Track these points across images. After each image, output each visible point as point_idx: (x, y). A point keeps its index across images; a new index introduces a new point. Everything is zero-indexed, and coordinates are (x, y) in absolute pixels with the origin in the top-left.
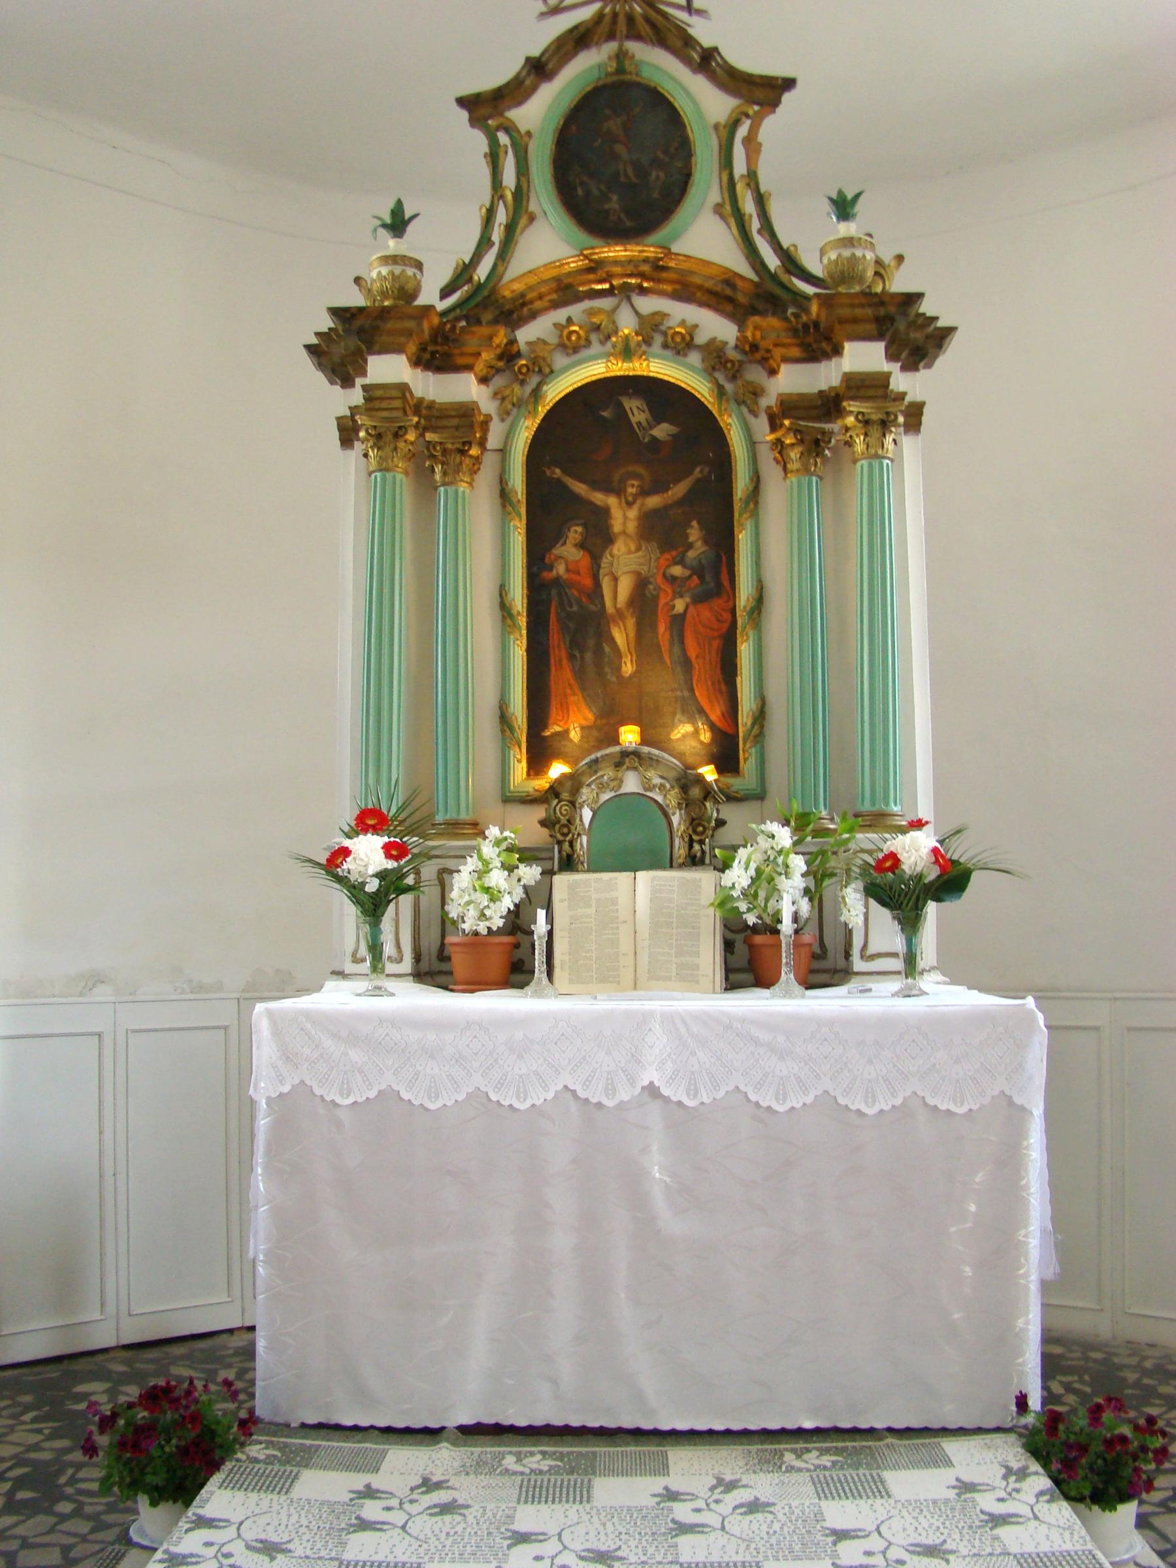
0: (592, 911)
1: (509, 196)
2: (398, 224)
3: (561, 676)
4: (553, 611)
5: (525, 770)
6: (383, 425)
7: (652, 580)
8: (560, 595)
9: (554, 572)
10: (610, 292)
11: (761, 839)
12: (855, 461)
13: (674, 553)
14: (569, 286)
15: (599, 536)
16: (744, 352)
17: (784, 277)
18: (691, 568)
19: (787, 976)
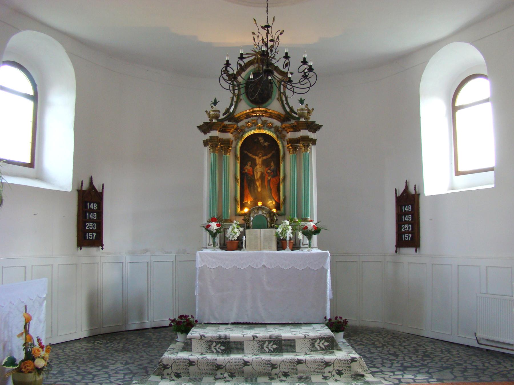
2: (215, 103)
3: (247, 191)
6: (212, 143)
15: (254, 165)
17: (290, 113)
19: (288, 247)
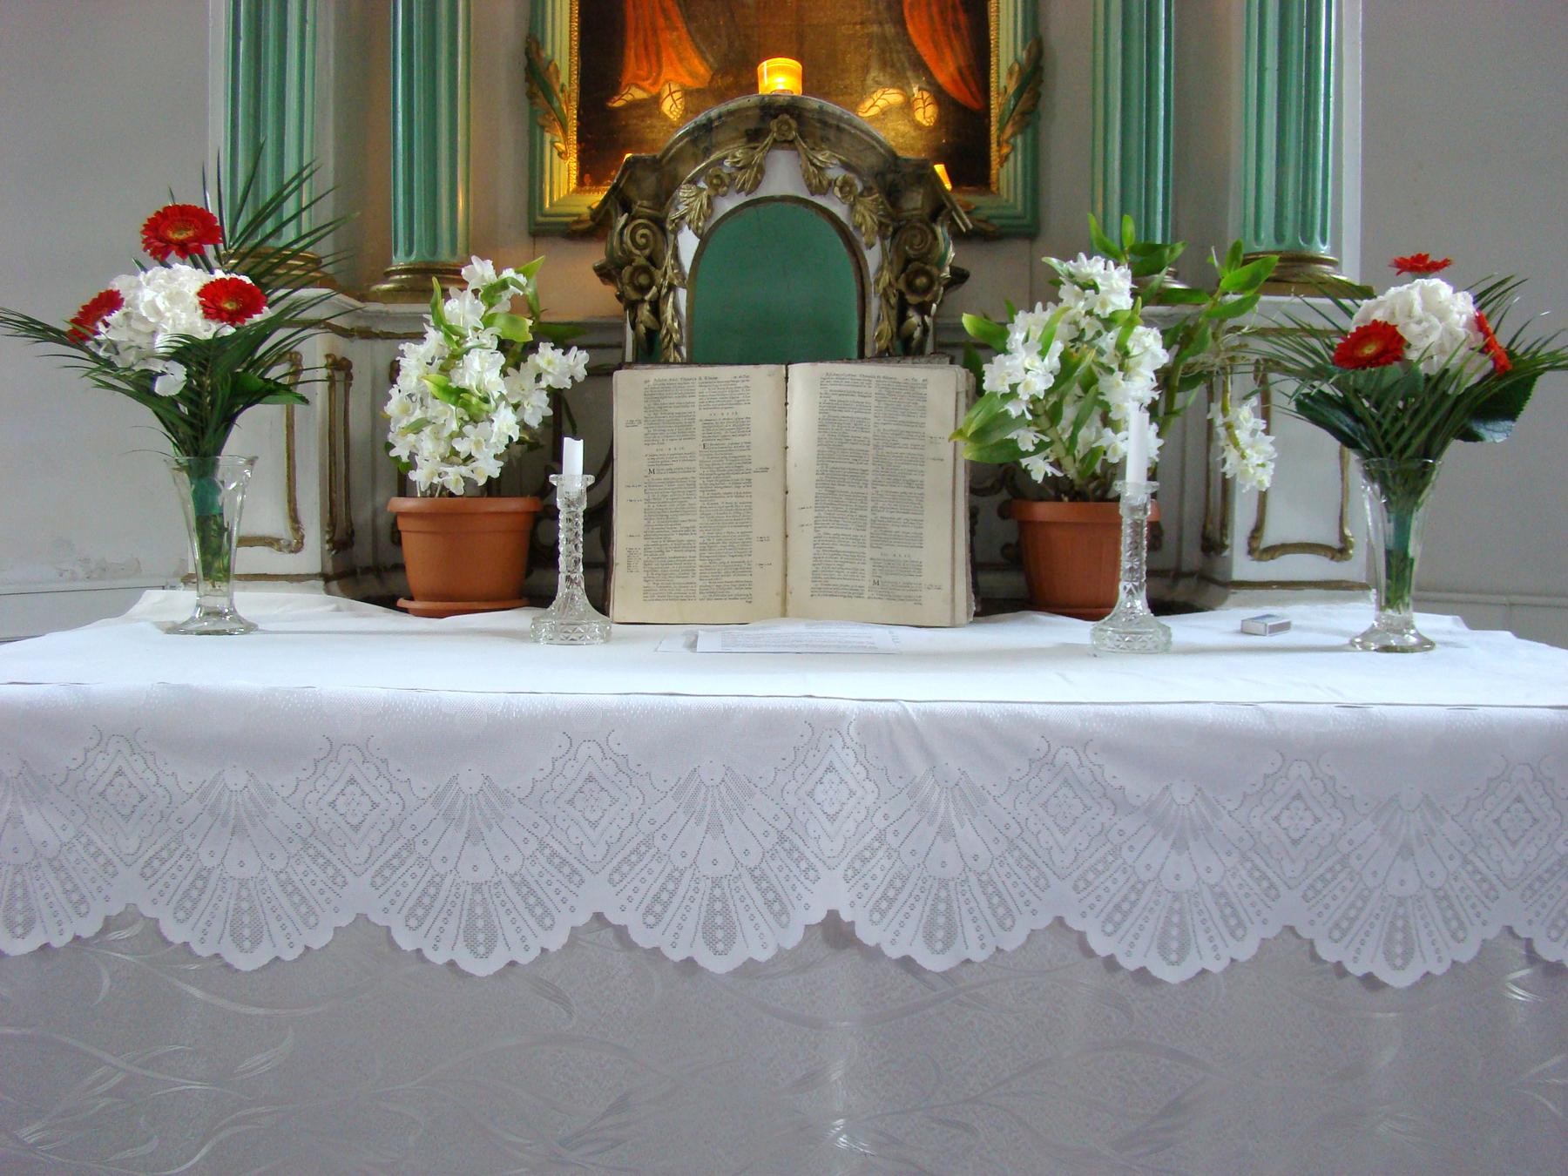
0: (694, 446)
5: (574, 174)
11: (1067, 292)
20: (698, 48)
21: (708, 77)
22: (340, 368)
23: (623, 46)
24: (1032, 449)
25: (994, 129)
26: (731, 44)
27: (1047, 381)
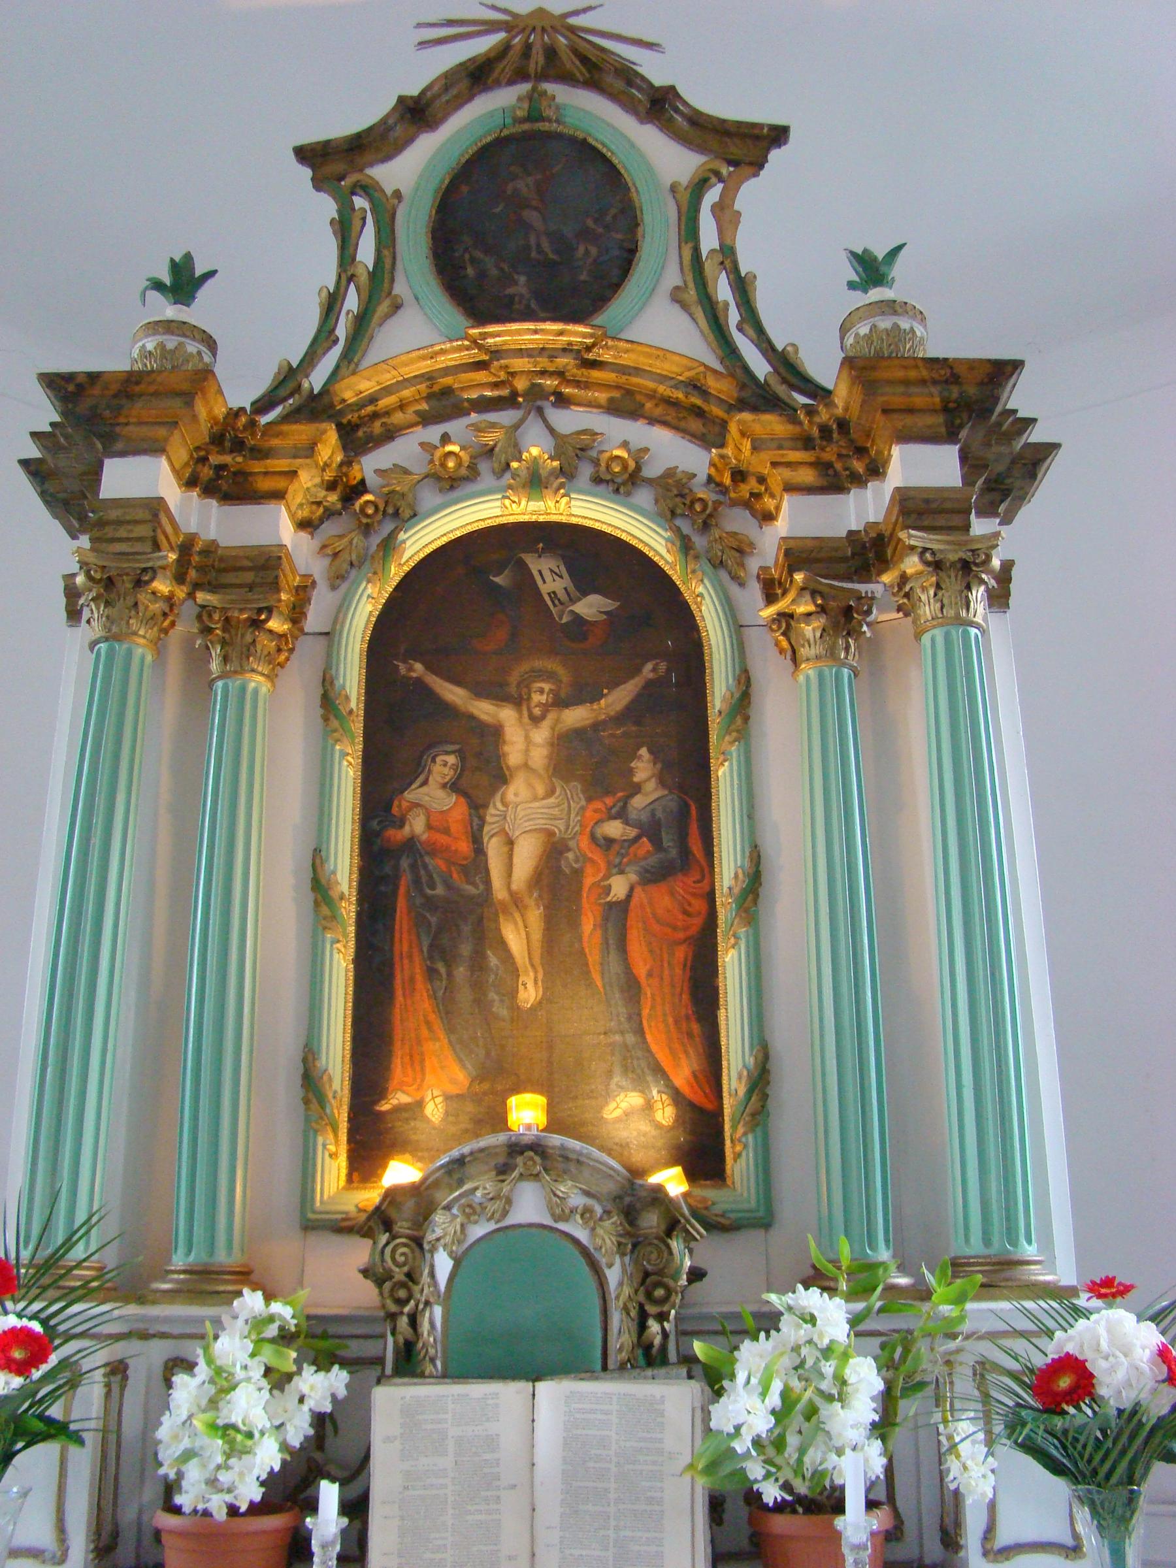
1: (363, 278)
3: (414, 1008)
4: (402, 890)
5: (344, 1172)
6: (119, 570)
7: (572, 844)
8: (414, 867)
9: (407, 828)
10: (509, 402)
12: (918, 636)
13: (609, 801)
14: (447, 392)
15: (483, 771)
16: (722, 490)
17: (781, 390)
18: (638, 825)
20: (458, 1056)
21: (467, 1083)
22: (118, 1370)
23: (389, 1055)
24: (760, 1478)
25: (727, 1127)
26: (488, 1054)
27: (769, 1422)
